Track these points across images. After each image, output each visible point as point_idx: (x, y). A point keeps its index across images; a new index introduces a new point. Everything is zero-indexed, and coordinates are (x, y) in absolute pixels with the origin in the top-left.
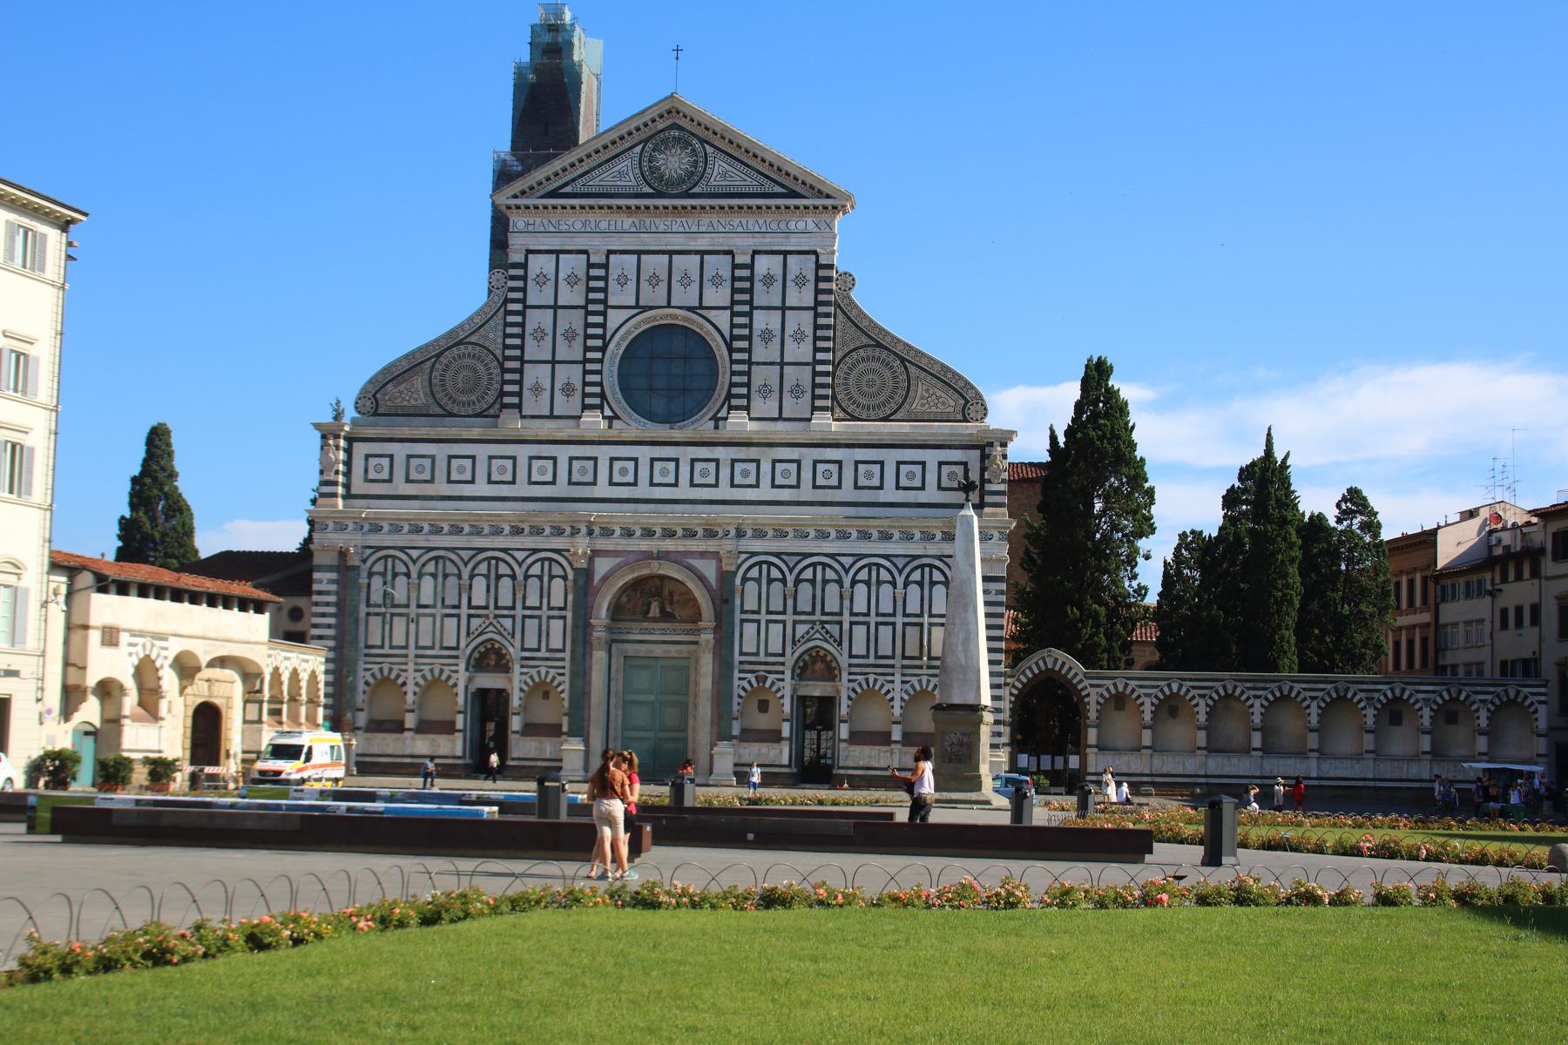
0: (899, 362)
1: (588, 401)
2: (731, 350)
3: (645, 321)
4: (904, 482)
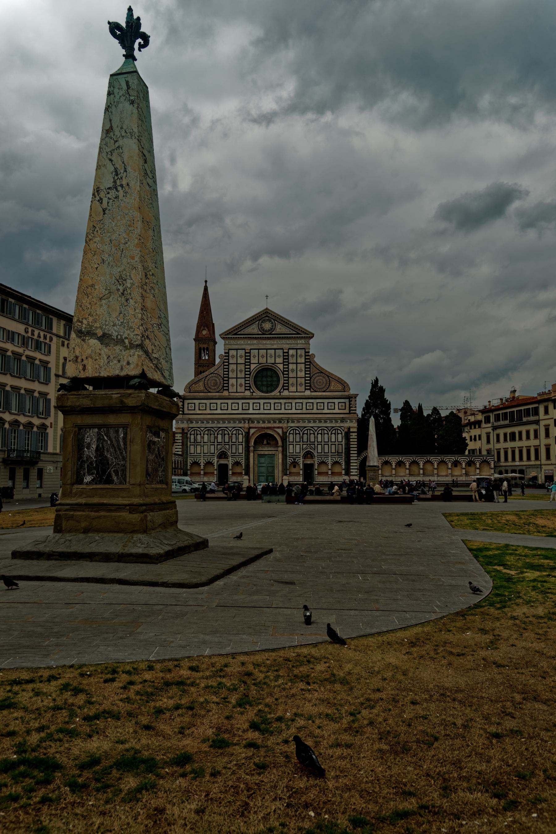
1: (246, 388)
2: (283, 374)
3: (261, 367)
4: (329, 408)
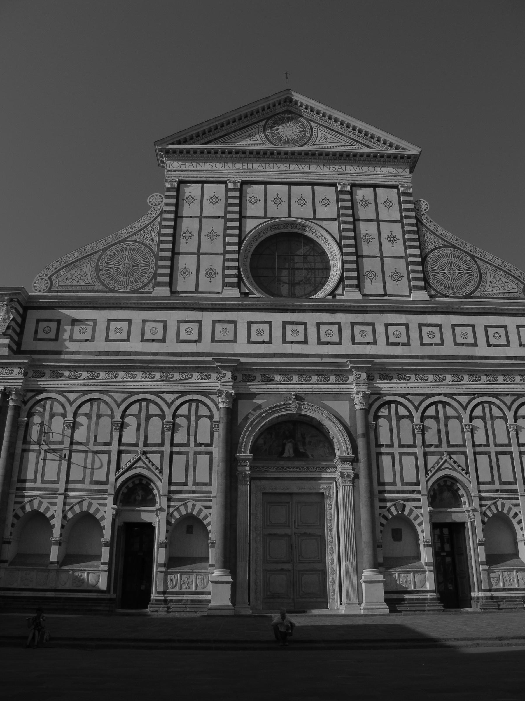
0: (469, 258)
1: (227, 280)
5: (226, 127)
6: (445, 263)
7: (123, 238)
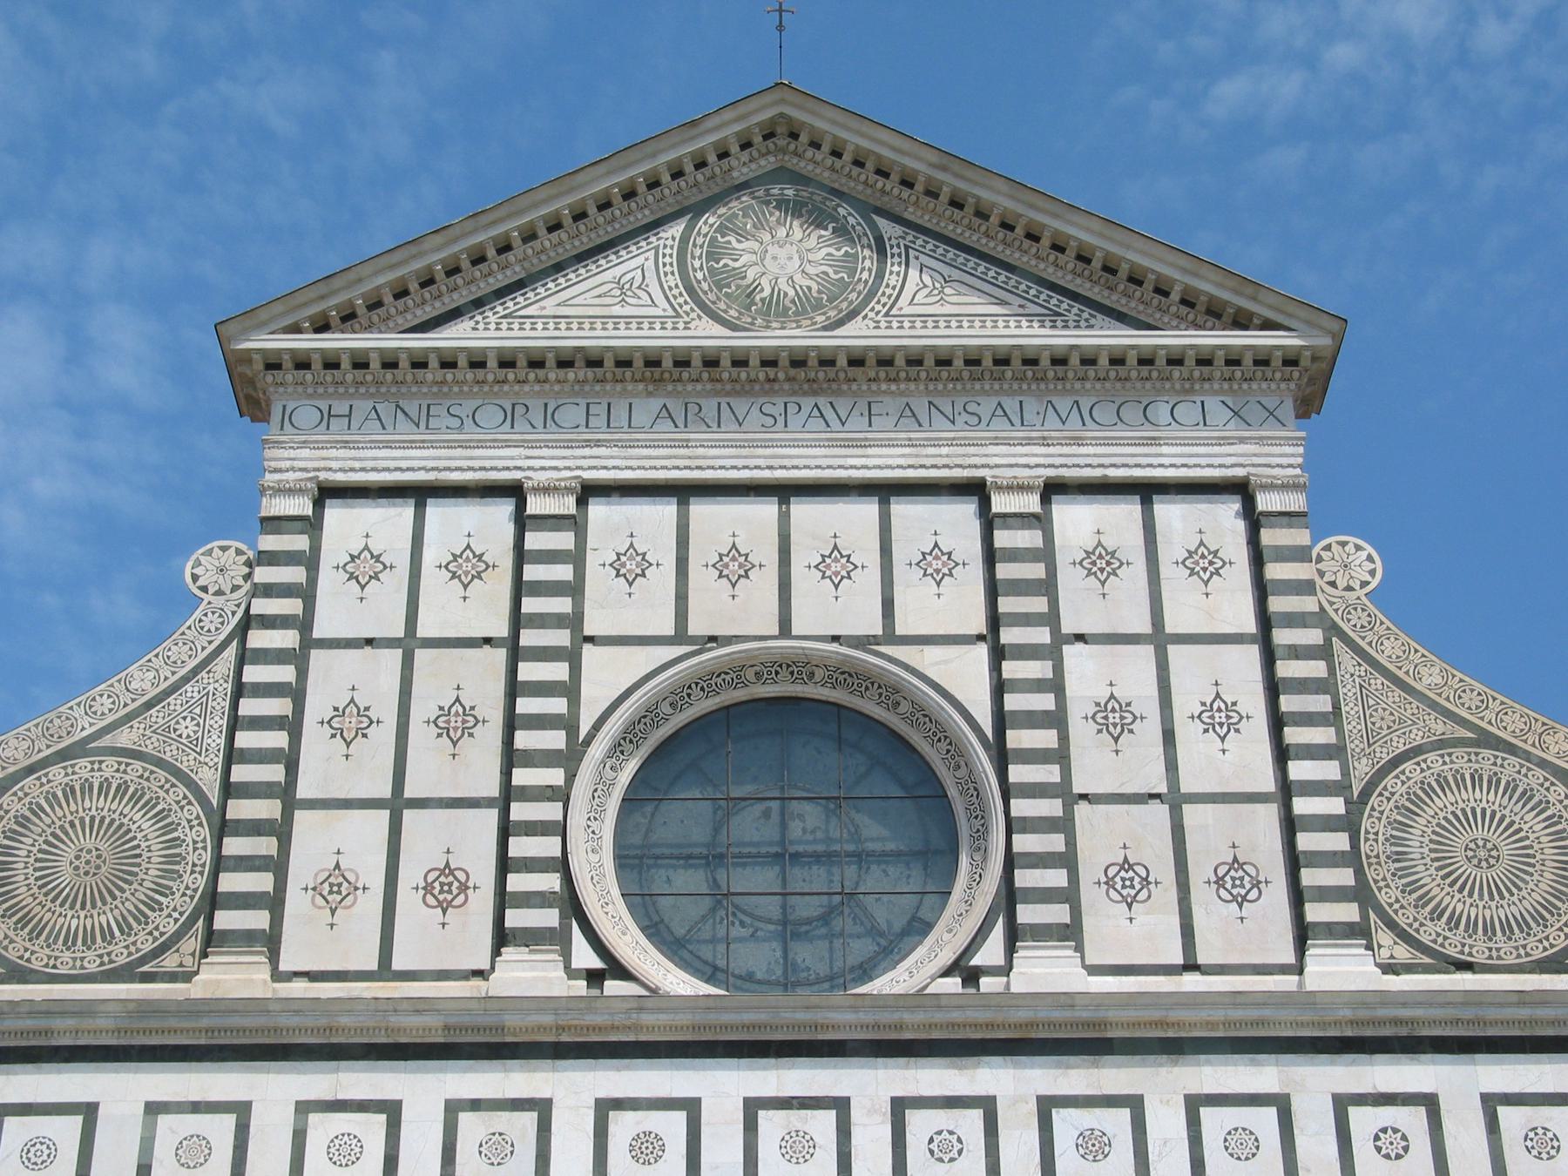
1: (514, 918)
2: (1002, 757)
3: (706, 681)
5: (519, 250)
6: (1451, 817)
7: (76, 738)
